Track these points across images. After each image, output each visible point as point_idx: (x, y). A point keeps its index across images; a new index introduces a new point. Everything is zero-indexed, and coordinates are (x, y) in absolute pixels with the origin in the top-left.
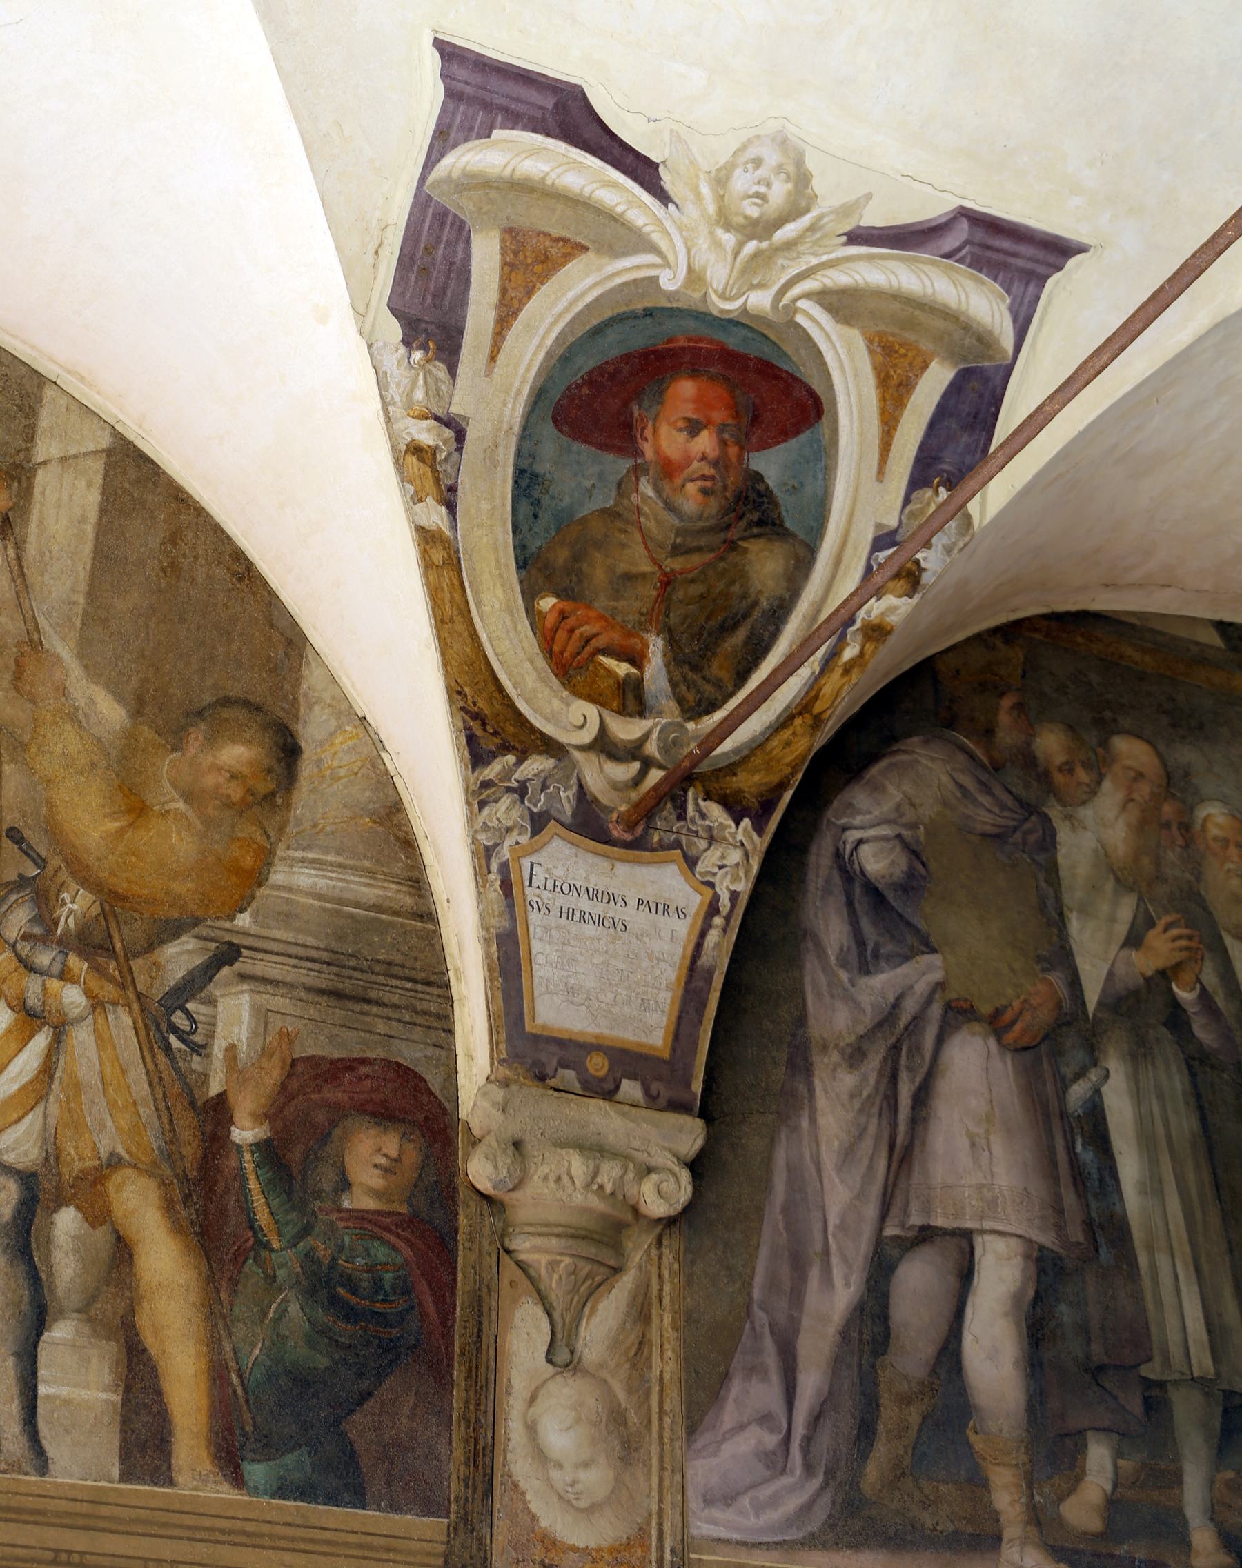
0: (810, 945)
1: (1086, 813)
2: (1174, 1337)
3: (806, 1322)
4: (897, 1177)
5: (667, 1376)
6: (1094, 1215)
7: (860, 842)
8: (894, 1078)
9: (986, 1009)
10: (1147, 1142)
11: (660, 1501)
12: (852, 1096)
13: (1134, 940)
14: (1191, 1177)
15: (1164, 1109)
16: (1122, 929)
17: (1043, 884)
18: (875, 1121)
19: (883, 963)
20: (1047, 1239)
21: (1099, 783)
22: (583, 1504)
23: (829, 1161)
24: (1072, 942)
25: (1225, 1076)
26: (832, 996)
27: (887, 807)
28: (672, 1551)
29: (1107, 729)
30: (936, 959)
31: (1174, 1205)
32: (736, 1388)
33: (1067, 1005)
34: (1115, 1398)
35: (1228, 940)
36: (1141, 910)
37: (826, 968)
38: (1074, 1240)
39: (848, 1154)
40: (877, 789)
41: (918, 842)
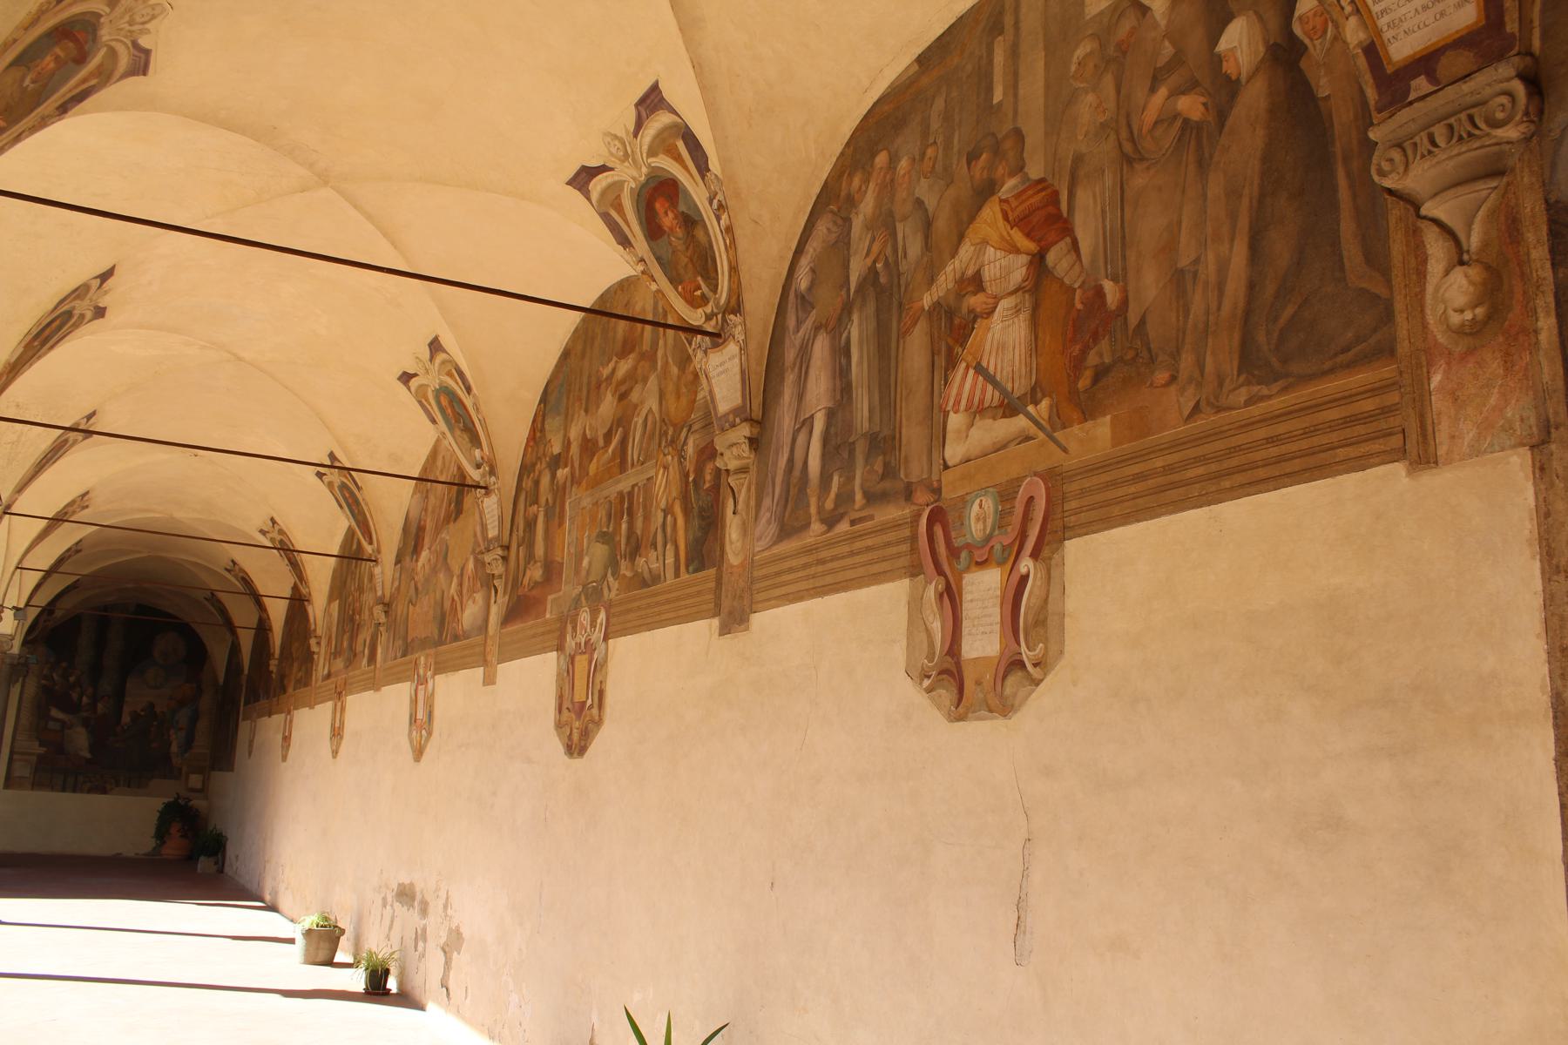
20: (830, 405)
35: (897, 224)
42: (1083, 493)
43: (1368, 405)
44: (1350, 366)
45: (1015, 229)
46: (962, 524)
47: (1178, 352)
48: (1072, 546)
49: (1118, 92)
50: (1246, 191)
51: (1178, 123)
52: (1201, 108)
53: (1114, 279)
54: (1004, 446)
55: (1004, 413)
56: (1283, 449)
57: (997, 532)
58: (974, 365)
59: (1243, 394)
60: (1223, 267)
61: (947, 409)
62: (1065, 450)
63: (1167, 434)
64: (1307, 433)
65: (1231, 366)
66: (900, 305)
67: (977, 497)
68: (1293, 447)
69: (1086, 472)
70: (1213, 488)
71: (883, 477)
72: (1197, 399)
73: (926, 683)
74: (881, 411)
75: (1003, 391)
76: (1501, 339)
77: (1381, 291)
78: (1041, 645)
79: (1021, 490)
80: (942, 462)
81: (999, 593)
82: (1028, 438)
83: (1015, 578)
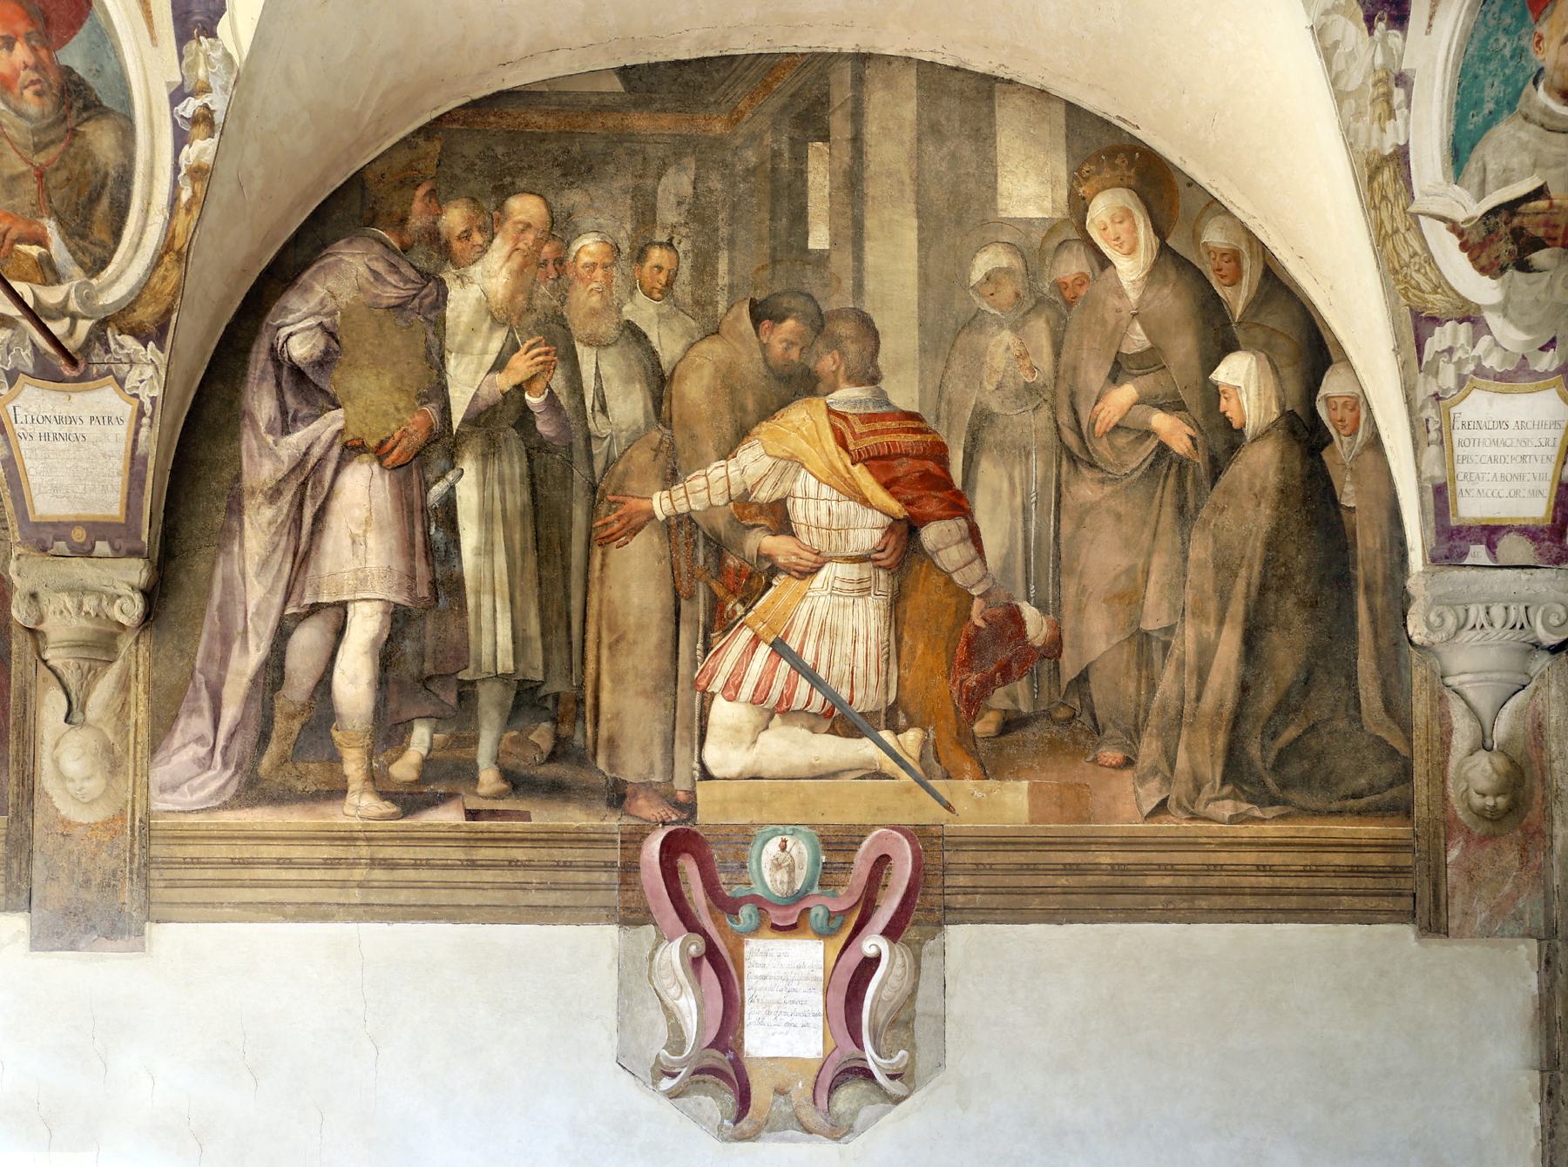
0: (247, 421)
1: (476, 271)
2: (486, 649)
3: (229, 677)
4: (298, 571)
5: (140, 722)
6: (438, 576)
7: (290, 335)
8: (301, 506)
9: (373, 443)
10: (486, 518)
11: (134, 793)
12: (270, 524)
13: (499, 365)
14: (517, 537)
15: (503, 491)
16: (490, 359)
17: (431, 337)
18: (285, 538)
19: (299, 424)
20: (401, 599)
21: (491, 242)
22: (86, 800)
23: (251, 569)
26: (261, 456)
27: (313, 302)
28: (141, 821)
29: (503, 192)
30: (339, 413)
31: (501, 560)
32: (182, 723)
33: (437, 427)
34: (438, 696)
35: (579, 348)
37: (258, 436)
39: (264, 564)
40: (308, 289)
41: (335, 325)
42: (979, 870)
43: (1379, 860)
44: (1361, 813)
45: (859, 465)
46: (744, 867)
47: (1137, 731)
48: (958, 936)
49: (1057, 355)
50: (1243, 572)
51: (1151, 445)
52: (1189, 443)
53: (1041, 606)
54: (834, 775)
55: (832, 726)
56: (1278, 881)
57: (816, 890)
58: (771, 640)
59: (1227, 808)
60: (1206, 653)
62: (948, 807)
63: (1119, 827)
64: (1308, 871)
65: (1213, 771)
66: (593, 489)
67: (775, 833)
68: (1291, 882)
70: (1185, 905)
71: (553, 757)
72: (1164, 796)
73: (667, 1084)
74: (546, 649)
75: (830, 695)
76: (1519, 833)
77: (1398, 744)
78: (902, 1052)
79: (865, 843)
80: (697, 765)
81: (821, 974)
82: (879, 775)
83: (852, 960)
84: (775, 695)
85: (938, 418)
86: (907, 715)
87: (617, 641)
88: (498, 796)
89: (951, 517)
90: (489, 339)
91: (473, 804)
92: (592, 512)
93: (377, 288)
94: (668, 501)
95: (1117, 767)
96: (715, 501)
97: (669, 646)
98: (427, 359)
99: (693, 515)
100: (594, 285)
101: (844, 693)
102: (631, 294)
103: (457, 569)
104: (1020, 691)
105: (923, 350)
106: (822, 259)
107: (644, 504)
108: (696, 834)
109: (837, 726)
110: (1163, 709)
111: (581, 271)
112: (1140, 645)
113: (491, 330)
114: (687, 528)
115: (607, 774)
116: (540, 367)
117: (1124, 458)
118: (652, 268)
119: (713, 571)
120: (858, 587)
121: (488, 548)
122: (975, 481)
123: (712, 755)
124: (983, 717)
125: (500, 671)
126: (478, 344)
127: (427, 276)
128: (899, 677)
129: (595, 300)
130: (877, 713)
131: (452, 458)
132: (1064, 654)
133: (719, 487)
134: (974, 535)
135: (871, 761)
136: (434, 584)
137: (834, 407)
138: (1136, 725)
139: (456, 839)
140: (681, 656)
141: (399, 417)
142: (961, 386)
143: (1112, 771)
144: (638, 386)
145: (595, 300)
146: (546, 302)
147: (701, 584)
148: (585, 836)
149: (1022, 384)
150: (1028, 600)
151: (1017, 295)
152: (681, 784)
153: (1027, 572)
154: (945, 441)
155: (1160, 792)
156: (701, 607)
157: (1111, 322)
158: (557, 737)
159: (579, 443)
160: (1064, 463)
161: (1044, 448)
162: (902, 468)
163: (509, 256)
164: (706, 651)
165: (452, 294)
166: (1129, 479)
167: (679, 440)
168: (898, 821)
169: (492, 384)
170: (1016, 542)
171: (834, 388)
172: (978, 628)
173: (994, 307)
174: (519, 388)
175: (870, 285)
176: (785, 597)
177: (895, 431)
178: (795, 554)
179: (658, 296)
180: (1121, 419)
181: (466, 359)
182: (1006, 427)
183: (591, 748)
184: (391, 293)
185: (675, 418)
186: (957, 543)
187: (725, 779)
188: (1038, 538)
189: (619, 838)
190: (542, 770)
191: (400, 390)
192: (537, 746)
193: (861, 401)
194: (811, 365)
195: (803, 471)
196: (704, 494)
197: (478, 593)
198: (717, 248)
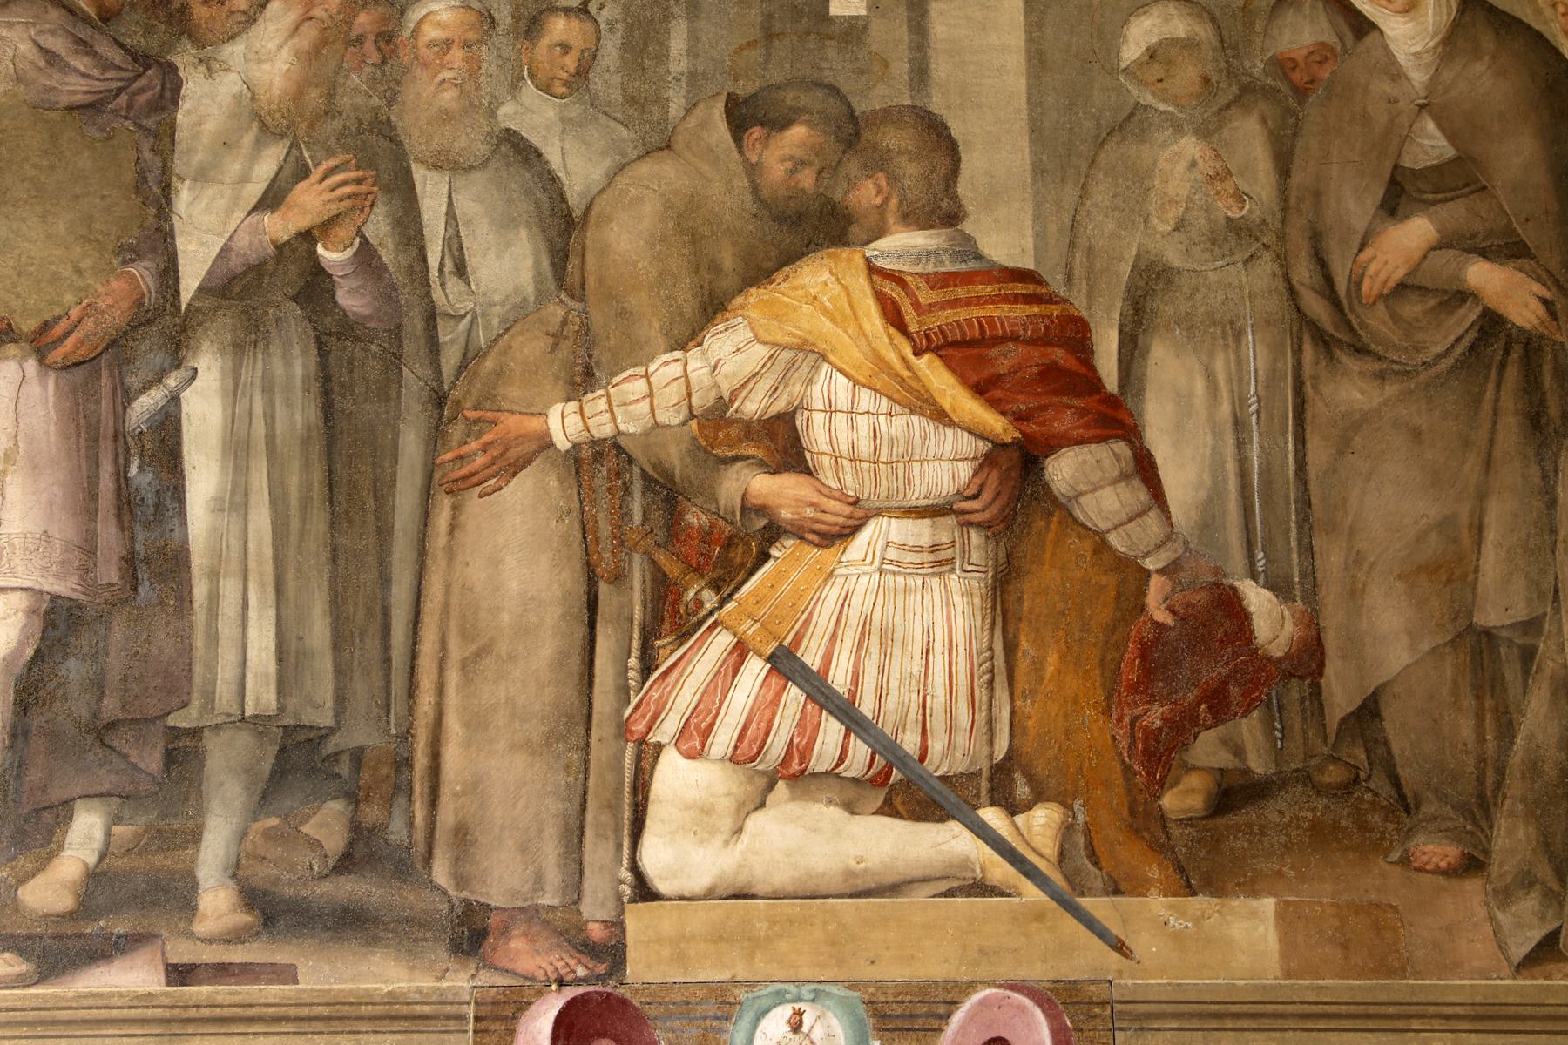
1: (234, 52)
6: (139, 547)
9: (29, 325)
10: (236, 449)
13: (272, 199)
14: (294, 480)
15: (270, 404)
16: (255, 190)
17: (147, 155)
20: (63, 587)
24: (175, 219)
25: (373, 347)
31: (261, 520)
34: (125, 757)
35: (419, 173)
36: (292, 159)
38: (104, 582)
45: (926, 357)
51: (1470, 314)
52: (1541, 310)
53: (1279, 587)
54: (893, 889)
58: (769, 650)
61: (653, 738)
62: (1120, 947)
63: (1461, 986)
66: (439, 399)
67: (780, 999)
69: (1201, 1016)
71: (346, 863)
74: (341, 671)
75: (884, 746)
79: (958, 1017)
80: (626, 874)
82: (981, 888)
84: (777, 746)
85: (1069, 278)
86: (1031, 780)
87: (478, 655)
88: (234, 937)
89: (1100, 439)
90: (253, 158)
91: (183, 952)
92: (436, 437)
93: (51, 77)
94: (578, 418)
95: (1450, 873)
96: (662, 418)
97: (575, 663)
98: (137, 190)
99: (622, 441)
100: (448, 74)
101: (910, 742)
102: (515, 85)
103: (177, 534)
104: (1246, 736)
105: (1039, 170)
106: (854, 30)
107: (534, 424)
108: (624, 1002)
109: (898, 801)
110: (1533, 767)
111: (424, 51)
112: (1477, 654)
113: (259, 145)
114: (613, 463)
115: (451, 892)
116: (347, 203)
117: (1419, 336)
118: (551, 47)
119: (660, 535)
120: (931, 558)
121: (238, 498)
122: (1142, 379)
123: (656, 855)
124: (1177, 782)
125: (249, 712)
126: (235, 167)
127: (141, 60)
128: (1013, 713)
129: (449, 97)
130: (972, 776)
131: (177, 350)
132: (1330, 669)
133: (674, 393)
134: (1145, 469)
135: (965, 863)
136: (130, 562)
137: (882, 263)
138: (1481, 796)
139: (144, 1021)
140: (597, 680)
141: (80, 283)
142: (1110, 226)
143: (1441, 880)
144: (524, 233)
145: (449, 97)
146: (359, 100)
147: (637, 558)
148: (405, 1010)
149: (1222, 222)
150: (1254, 576)
151: (1206, 81)
152: (594, 912)
153: (1248, 527)
154: (1084, 314)
155: (1543, 918)
156: (637, 596)
157: (1381, 119)
158: (356, 828)
159: (415, 324)
160: (1308, 347)
161: (1268, 323)
162: (1006, 359)
163: (297, 29)
164: (646, 670)
165: (189, 88)
166: (1432, 372)
167: (597, 320)
168: (1022, 973)
169: (257, 230)
170: (1225, 481)
171: (879, 233)
172: (1160, 626)
173: (1166, 101)
174: (307, 237)
175: (941, 69)
176: (794, 575)
177: (992, 300)
178: (812, 505)
179: (560, 90)
180: (1408, 274)
181: (210, 191)
182: (1196, 290)
183: (421, 848)
184: (76, 86)
185: (591, 283)
186: (1115, 482)
187: (682, 898)
188: (1266, 471)
189: (471, 1011)
190: (325, 887)
191: (85, 239)
192: (315, 844)
193: (928, 254)
194: (838, 196)
195: (825, 365)
196: (644, 406)
197: (214, 575)
198: (667, 16)
